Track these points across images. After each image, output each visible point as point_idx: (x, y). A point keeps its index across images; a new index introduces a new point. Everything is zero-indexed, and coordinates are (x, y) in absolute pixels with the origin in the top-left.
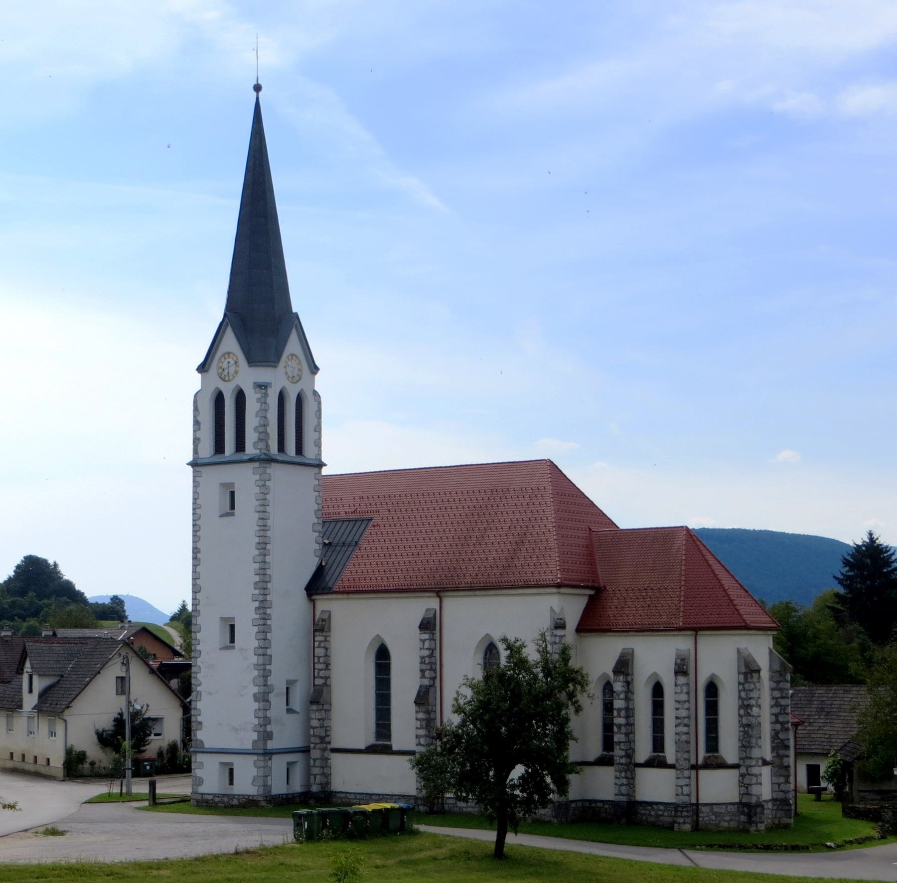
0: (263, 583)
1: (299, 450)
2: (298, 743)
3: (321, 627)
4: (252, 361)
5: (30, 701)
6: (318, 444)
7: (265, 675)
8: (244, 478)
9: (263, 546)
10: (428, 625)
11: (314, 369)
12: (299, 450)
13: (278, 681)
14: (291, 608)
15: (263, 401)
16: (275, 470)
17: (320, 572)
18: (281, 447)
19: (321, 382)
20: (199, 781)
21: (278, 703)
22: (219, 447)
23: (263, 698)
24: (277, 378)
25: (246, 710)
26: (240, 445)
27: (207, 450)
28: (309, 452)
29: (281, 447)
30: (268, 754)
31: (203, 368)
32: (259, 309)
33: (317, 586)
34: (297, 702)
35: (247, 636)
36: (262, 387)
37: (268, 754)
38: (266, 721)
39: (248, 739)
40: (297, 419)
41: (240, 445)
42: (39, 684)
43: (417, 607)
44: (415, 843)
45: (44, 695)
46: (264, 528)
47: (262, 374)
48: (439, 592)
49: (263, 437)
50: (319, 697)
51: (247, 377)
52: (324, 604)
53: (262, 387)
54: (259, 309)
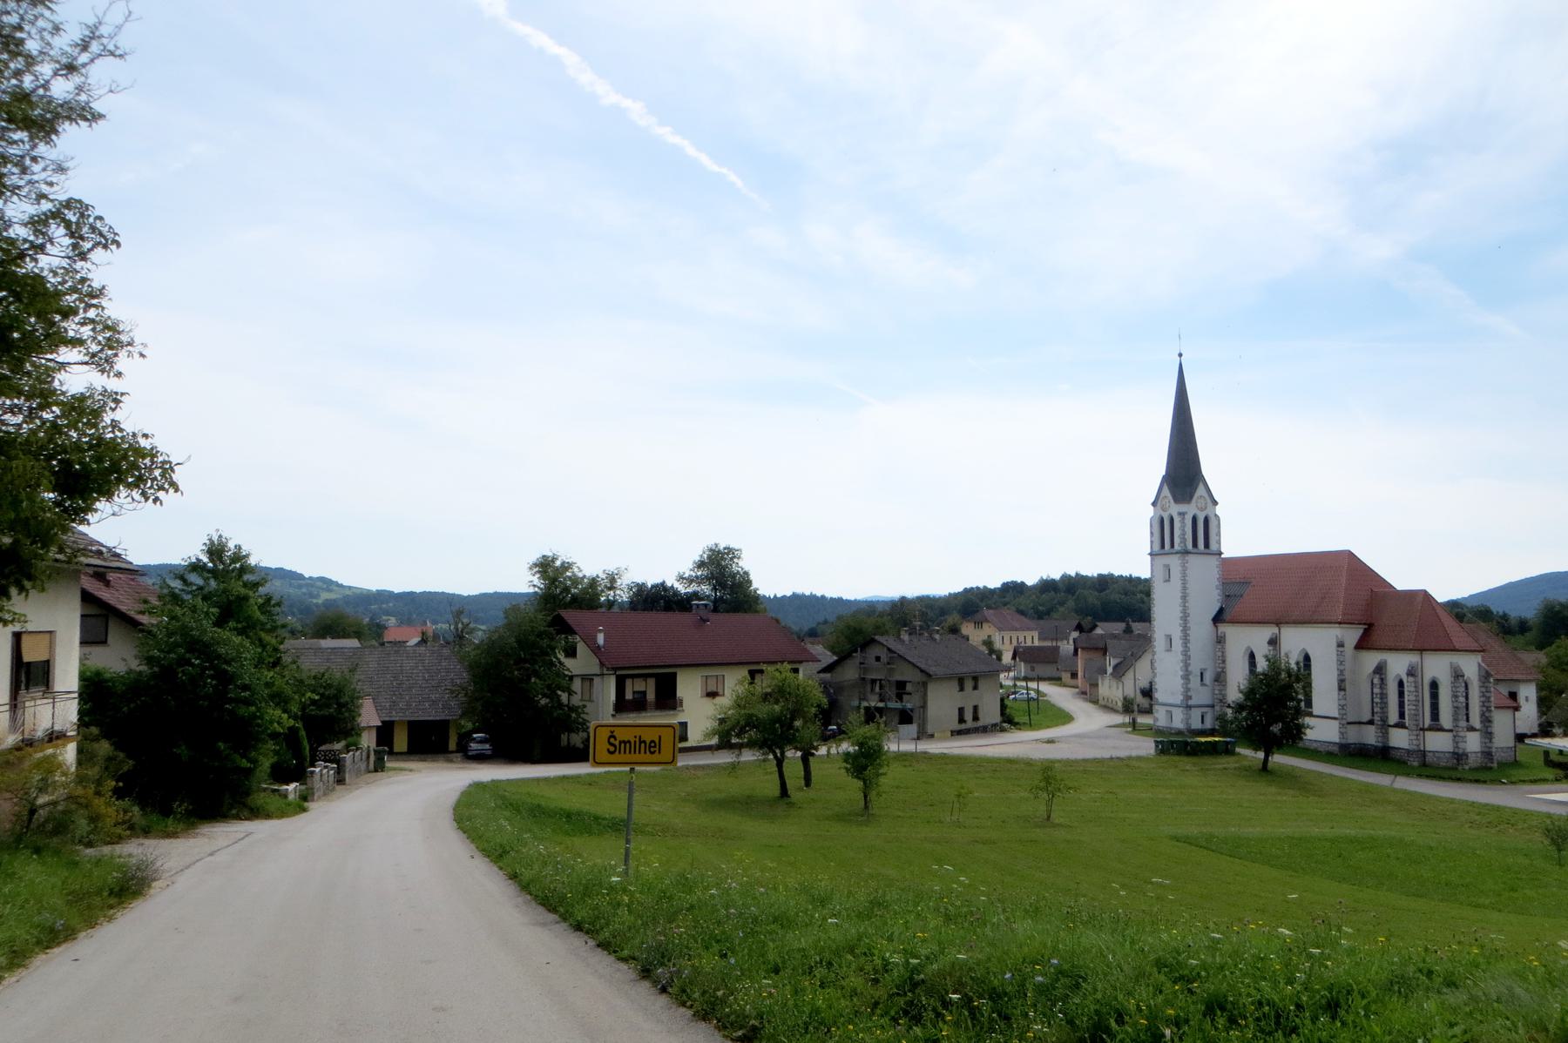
0: (1185, 617)
1: (1207, 545)
2: (1209, 702)
3: (1220, 640)
4: (1177, 501)
5: (1110, 670)
6: (1219, 542)
7: (1186, 666)
8: (1174, 562)
9: (1184, 597)
10: (1273, 642)
11: (1215, 503)
12: (1207, 545)
13: (1195, 668)
14: (1202, 629)
15: (1183, 521)
16: (1190, 558)
17: (1221, 611)
18: (1195, 544)
19: (1219, 510)
20: (1156, 720)
21: (1195, 680)
22: (1163, 546)
23: (1186, 677)
24: (1191, 509)
25: (1178, 682)
26: (1172, 545)
27: (1157, 547)
28: (1213, 547)
29: (1195, 544)
30: (1189, 707)
31: (1154, 504)
32: (1184, 473)
33: (1218, 618)
34: (1208, 678)
35: (1178, 644)
36: (1182, 514)
37: (1189, 707)
38: (1188, 690)
39: (1178, 699)
40: (1204, 533)
41: (1172, 545)
42: (1114, 662)
43: (1267, 632)
44: (1232, 759)
45: (1115, 667)
46: (1184, 588)
47: (1183, 508)
48: (1278, 624)
49: (1184, 540)
50: (1220, 678)
51: (1175, 509)
52: (1223, 628)
53: (1182, 514)
54: (1184, 473)
